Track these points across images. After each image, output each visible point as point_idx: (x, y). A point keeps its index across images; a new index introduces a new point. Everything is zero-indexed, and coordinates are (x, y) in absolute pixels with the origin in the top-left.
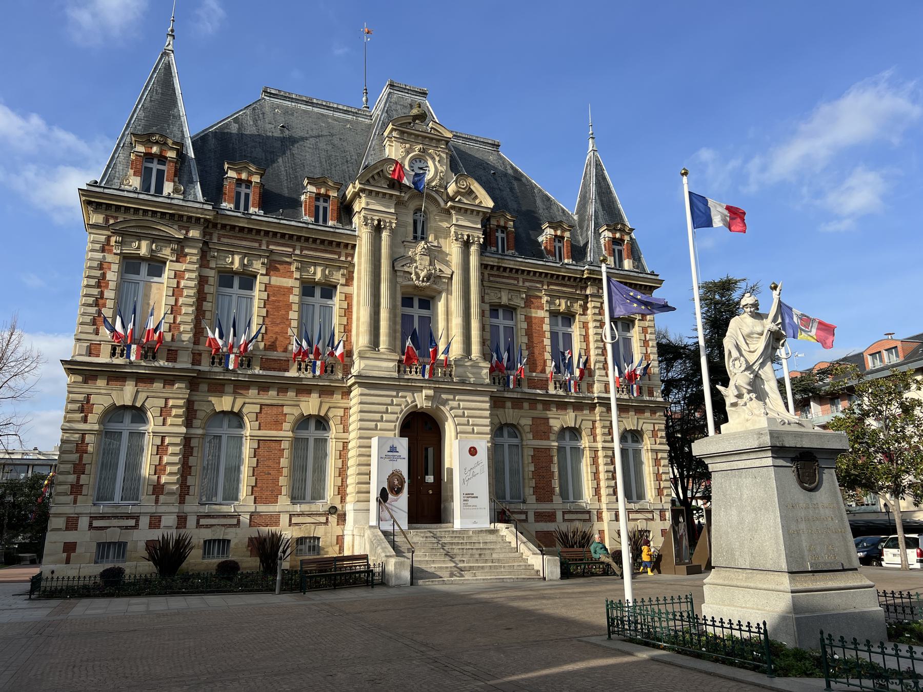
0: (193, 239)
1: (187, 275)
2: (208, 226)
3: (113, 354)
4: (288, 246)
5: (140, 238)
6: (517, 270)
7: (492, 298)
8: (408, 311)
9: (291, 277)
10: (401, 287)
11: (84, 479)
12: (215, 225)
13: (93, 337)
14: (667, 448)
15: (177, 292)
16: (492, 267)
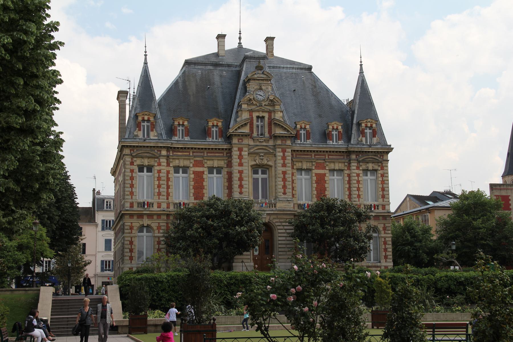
0: (164, 156)
1: (162, 171)
2: (168, 149)
3: (138, 206)
4: (201, 152)
5: (142, 157)
6: (311, 151)
7: (298, 165)
8: (255, 176)
9: (204, 167)
10: (252, 166)
11: (133, 254)
12: (171, 148)
13: (131, 200)
14: (391, 235)
15: (159, 179)
16: (298, 151)
